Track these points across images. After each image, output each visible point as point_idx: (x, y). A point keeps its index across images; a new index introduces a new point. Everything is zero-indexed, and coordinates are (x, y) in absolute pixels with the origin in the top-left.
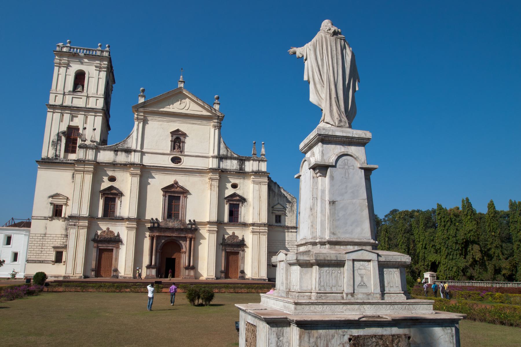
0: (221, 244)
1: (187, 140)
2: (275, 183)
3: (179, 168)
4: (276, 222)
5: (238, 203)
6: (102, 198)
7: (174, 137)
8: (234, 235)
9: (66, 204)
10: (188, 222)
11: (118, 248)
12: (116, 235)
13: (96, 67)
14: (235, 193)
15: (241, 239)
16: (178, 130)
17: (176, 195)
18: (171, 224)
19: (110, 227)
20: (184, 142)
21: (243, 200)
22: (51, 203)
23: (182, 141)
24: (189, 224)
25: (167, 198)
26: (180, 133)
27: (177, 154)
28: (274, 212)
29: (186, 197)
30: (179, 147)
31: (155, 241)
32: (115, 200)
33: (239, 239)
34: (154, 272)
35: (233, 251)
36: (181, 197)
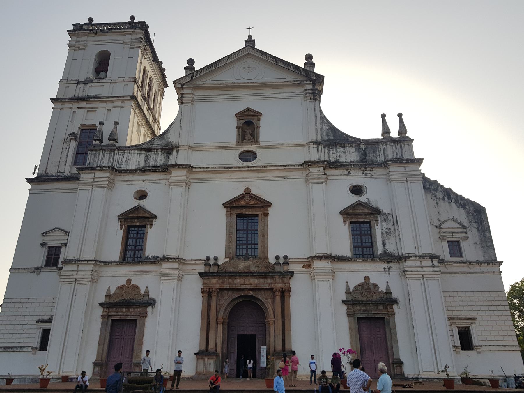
0: (343, 302)
1: (263, 123)
3: (251, 167)
4: (452, 255)
5: (367, 220)
6: (121, 229)
8: (369, 282)
9: (66, 244)
12: (142, 292)
14: (359, 201)
15: (385, 291)
16: (248, 110)
17: (250, 213)
19: (132, 278)
20: (258, 127)
21: (376, 212)
22: (43, 245)
23: (255, 125)
24: (275, 264)
26: (252, 113)
28: (443, 234)
29: (266, 215)
30: (252, 135)
31: (214, 299)
35: (370, 316)
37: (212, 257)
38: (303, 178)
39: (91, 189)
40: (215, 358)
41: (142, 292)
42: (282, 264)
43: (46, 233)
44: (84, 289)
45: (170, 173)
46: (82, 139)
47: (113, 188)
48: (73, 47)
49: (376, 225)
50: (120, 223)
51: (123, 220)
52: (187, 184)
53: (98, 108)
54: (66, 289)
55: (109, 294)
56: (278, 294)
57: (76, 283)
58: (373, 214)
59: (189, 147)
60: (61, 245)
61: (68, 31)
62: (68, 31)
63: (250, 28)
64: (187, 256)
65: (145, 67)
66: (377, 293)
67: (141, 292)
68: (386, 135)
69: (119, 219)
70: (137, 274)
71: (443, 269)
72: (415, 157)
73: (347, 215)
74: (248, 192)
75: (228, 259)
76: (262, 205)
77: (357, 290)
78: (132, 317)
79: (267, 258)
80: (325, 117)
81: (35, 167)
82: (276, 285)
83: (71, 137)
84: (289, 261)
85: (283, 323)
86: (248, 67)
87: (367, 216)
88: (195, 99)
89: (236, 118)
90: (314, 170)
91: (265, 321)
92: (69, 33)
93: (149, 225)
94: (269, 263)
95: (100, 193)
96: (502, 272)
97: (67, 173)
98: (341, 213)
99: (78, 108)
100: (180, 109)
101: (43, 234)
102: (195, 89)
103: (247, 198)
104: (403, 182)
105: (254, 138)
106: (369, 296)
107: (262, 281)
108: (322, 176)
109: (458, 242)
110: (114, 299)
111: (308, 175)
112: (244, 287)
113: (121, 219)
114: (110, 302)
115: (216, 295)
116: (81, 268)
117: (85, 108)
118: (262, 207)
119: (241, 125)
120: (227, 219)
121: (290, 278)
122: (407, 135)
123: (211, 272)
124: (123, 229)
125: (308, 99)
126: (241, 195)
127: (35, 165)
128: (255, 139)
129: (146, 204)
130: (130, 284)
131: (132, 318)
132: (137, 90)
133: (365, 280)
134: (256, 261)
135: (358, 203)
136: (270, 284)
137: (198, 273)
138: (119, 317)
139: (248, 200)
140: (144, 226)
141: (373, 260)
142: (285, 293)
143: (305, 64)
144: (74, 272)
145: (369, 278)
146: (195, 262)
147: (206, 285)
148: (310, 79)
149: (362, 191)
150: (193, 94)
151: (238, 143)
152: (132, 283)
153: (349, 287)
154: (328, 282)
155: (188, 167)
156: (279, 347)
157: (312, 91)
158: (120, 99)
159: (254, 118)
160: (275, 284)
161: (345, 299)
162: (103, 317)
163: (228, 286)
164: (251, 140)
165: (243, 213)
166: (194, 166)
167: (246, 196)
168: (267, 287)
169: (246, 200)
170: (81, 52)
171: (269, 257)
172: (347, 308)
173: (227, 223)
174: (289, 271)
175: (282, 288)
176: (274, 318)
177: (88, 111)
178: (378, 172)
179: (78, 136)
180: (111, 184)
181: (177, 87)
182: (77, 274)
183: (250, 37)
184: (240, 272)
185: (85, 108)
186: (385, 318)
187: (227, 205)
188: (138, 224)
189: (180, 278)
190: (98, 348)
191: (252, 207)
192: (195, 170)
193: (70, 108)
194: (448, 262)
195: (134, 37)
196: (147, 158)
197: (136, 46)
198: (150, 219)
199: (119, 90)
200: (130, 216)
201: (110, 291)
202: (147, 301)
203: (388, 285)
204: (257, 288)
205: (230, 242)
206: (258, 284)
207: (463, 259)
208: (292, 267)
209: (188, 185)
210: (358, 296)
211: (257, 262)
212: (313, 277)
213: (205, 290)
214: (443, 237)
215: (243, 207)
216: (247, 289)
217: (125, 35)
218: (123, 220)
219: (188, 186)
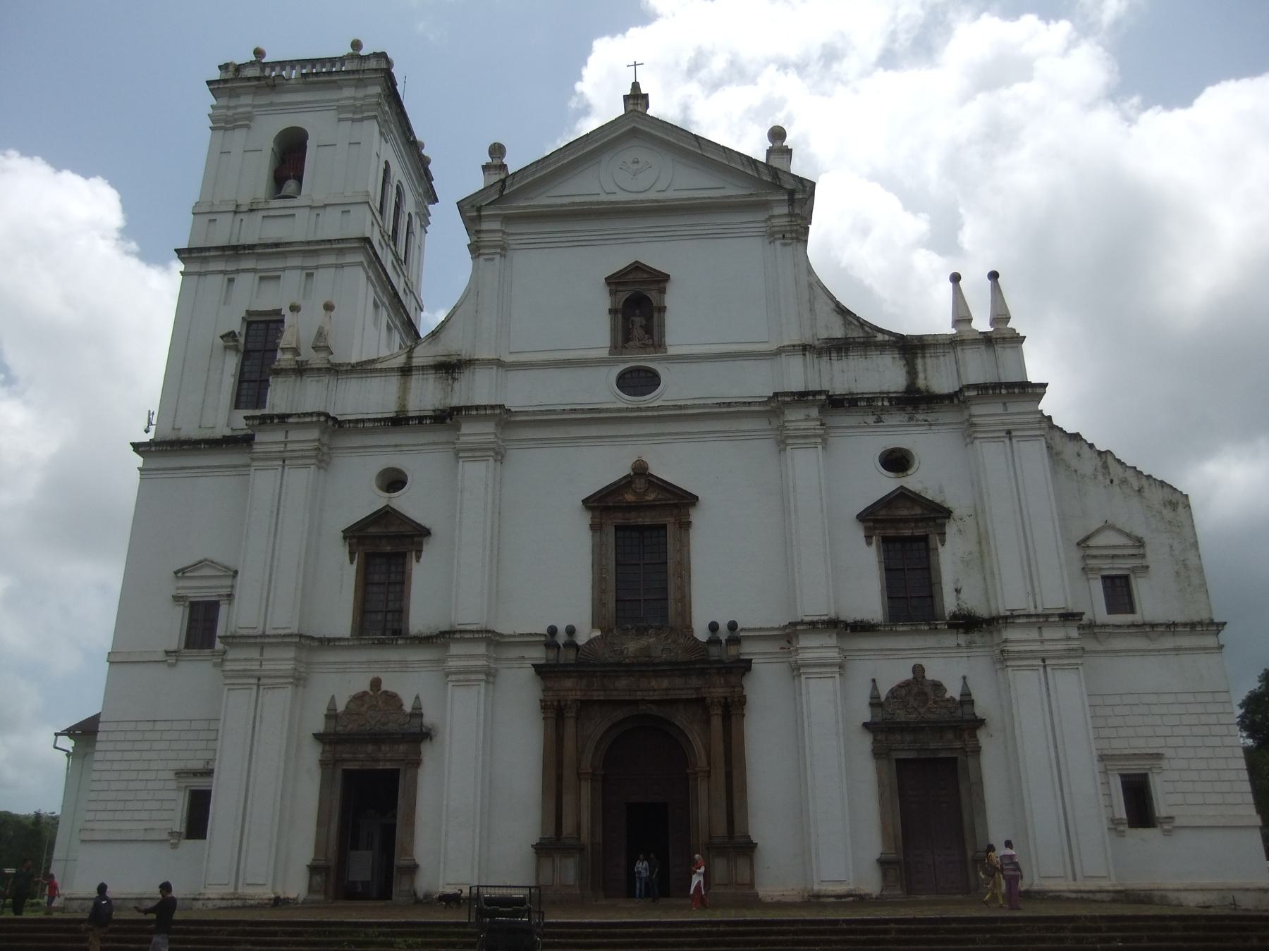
0: (866, 725)
2: (1076, 437)
4: (1112, 609)
5: (919, 532)
6: (352, 562)
7: (623, 296)
8: (924, 677)
9: (230, 596)
10: (702, 634)
11: (417, 763)
12: (408, 708)
13: (340, 109)
14: (902, 487)
15: (958, 698)
16: (637, 267)
17: (648, 521)
18: (632, 646)
19: (382, 676)
20: (662, 309)
21: (937, 514)
23: (655, 304)
24: (710, 642)
25: (611, 539)
26: (645, 276)
27: (636, 360)
29: (685, 525)
30: (648, 330)
32: (404, 564)
33: (947, 696)
34: (568, 871)
36: (670, 529)
37: (562, 629)
38: (772, 433)
39: (280, 468)
40: (578, 855)
41: (408, 708)
42: (724, 642)
43: (183, 571)
44: (278, 701)
45: (457, 428)
46: (250, 346)
47: (328, 464)
48: (222, 124)
49: (939, 545)
50: (347, 550)
51: (354, 541)
52: (497, 454)
53: (284, 269)
54: (238, 702)
55: (333, 712)
56: (717, 712)
57: (261, 688)
58: (934, 519)
59: (499, 363)
60: (216, 599)
61: (209, 83)
62: (209, 83)
63: (635, 65)
64: (505, 627)
65: (387, 163)
66: (942, 703)
67: (404, 708)
68: (963, 327)
69: (345, 538)
70: (392, 666)
71: (1090, 645)
72: (1029, 381)
73: (876, 521)
74: (640, 470)
75: (598, 633)
76: (676, 502)
77: (894, 698)
78: (387, 764)
79: (689, 628)
80: (819, 282)
81: (149, 415)
82: (712, 690)
83: (228, 342)
84: (741, 634)
85: (729, 776)
86: (634, 162)
87: (920, 524)
88: (510, 242)
89: (608, 289)
90: (797, 418)
91: (688, 771)
92: (212, 87)
93: (414, 554)
94: (696, 640)
95: (300, 479)
96: (1222, 647)
97: (222, 431)
98: (862, 517)
99: (238, 271)
100: (475, 269)
101: (176, 573)
102: (508, 219)
103: (640, 485)
104: (1002, 439)
105: (652, 337)
106: (922, 710)
107: (679, 682)
108: (815, 429)
109: (1126, 578)
110: (345, 724)
111: (782, 428)
112: (639, 695)
113: (351, 538)
114: (337, 730)
115: (573, 715)
116: (268, 653)
117: (255, 270)
118: (675, 505)
119: (620, 306)
120: (593, 536)
121: (743, 674)
122: (1009, 326)
123: (562, 662)
124: (355, 562)
125: (779, 239)
126: (625, 477)
127: (149, 411)
128: (656, 338)
129: (404, 502)
130: (379, 690)
131: (389, 767)
132: (372, 222)
133: (914, 673)
134: (666, 635)
135: (899, 492)
136: (698, 689)
137: (532, 665)
138: (357, 763)
139: (642, 490)
140: (403, 556)
141: (935, 630)
142: (733, 708)
143: (769, 152)
144: (254, 663)
145: (923, 670)
146: (525, 641)
147: (551, 693)
148: (781, 188)
149: (908, 462)
150: (504, 233)
151: (616, 348)
152: (384, 687)
153: (878, 692)
154: (830, 681)
155: (502, 416)
156: (721, 829)
157: (787, 219)
158: (334, 246)
159: (651, 287)
160: (709, 688)
161: (868, 718)
162: (323, 764)
163: (600, 696)
164: (647, 342)
165: (632, 521)
166: (513, 409)
167: (637, 481)
168: (693, 695)
169: (638, 491)
170: (240, 135)
171: (693, 626)
172: (872, 740)
173: (593, 545)
174: (742, 657)
175: (726, 698)
176: (709, 764)
177: (262, 278)
178: (945, 416)
179: (242, 340)
180: (322, 458)
181: (468, 214)
182: (261, 666)
183: (636, 86)
184: (627, 661)
185: (255, 270)
186: (959, 759)
187: (593, 502)
188: (389, 548)
189: (490, 676)
190: (317, 832)
191: (651, 507)
192: (513, 419)
193: (221, 272)
194: (1104, 626)
195: (361, 93)
196: (404, 392)
197: (365, 115)
198: (416, 539)
199: (332, 226)
200: (369, 530)
201: (335, 705)
202: (419, 729)
203: (965, 684)
204: (669, 697)
205: (603, 592)
206: (670, 689)
207: (1135, 618)
208: (747, 650)
209: (499, 456)
210: (898, 711)
211: (667, 638)
212: (796, 670)
213: (549, 703)
214: (1092, 569)
215: (630, 508)
216: (644, 700)
217: (340, 88)
218: (354, 541)
219: (499, 458)
